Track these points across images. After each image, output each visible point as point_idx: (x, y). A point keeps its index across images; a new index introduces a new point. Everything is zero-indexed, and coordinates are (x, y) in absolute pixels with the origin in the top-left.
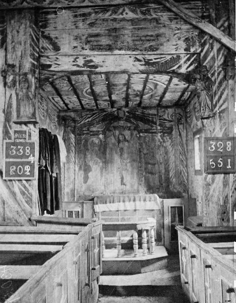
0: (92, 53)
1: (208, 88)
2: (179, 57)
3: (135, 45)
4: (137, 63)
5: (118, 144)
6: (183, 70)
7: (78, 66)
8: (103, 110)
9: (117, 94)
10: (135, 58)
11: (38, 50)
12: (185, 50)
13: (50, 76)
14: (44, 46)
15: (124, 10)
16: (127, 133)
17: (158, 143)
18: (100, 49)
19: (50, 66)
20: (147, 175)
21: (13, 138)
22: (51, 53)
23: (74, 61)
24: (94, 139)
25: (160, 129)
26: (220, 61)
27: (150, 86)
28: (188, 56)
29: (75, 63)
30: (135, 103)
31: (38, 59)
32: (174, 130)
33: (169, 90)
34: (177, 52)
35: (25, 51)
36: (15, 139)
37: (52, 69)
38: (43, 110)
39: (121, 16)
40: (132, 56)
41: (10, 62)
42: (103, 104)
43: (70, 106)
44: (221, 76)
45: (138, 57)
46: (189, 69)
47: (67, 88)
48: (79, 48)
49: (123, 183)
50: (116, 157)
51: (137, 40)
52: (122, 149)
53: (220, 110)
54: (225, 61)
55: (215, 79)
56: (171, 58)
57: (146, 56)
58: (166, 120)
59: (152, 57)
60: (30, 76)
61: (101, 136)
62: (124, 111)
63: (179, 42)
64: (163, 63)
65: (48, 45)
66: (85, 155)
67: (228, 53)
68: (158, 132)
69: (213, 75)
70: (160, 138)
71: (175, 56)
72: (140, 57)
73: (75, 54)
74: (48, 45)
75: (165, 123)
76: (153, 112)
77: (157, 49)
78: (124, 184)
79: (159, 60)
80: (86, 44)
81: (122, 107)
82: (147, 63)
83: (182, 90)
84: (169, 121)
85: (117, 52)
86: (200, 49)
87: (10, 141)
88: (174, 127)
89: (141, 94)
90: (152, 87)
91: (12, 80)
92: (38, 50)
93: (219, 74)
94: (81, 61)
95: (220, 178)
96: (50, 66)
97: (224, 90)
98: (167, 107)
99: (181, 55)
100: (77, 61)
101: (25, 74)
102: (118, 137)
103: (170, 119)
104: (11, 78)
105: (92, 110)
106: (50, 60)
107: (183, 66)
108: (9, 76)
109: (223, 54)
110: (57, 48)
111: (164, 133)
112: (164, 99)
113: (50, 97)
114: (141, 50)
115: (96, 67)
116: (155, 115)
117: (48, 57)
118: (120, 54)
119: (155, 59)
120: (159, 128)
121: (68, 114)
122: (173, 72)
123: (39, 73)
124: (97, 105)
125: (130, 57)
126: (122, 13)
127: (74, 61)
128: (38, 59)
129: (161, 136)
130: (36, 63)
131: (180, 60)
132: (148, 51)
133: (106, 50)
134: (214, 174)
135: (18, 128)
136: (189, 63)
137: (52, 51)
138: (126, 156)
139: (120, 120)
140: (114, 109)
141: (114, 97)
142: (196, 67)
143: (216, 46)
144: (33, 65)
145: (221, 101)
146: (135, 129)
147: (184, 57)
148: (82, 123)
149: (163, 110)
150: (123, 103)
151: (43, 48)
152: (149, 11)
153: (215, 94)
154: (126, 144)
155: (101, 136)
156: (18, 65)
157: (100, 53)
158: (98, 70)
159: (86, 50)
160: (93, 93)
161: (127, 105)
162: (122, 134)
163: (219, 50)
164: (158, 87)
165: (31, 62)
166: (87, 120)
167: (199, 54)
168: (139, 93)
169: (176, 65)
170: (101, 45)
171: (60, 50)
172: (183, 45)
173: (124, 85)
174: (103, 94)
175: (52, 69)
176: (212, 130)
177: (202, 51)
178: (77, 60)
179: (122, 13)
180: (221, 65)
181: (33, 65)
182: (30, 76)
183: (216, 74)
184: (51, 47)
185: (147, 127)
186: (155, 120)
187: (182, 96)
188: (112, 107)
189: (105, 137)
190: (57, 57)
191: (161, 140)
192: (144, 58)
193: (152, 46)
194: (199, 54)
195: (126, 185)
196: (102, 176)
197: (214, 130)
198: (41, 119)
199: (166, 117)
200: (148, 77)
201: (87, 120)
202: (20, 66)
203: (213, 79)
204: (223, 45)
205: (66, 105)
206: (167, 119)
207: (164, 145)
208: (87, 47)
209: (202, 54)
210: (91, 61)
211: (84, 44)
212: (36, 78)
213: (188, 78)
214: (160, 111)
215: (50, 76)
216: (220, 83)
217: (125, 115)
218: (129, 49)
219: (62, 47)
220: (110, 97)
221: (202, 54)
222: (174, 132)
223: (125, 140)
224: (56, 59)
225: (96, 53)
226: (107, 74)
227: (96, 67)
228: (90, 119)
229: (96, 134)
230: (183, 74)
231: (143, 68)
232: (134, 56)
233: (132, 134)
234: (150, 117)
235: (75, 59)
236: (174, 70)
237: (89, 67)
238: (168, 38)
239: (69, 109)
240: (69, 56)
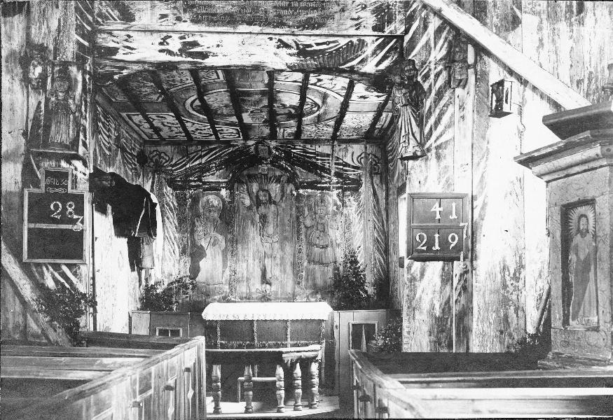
0: (195, 28)
1: (415, 101)
2: (362, 43)
3: (280, 16)
4: (284, 51)
5: (257, 208)
6: (370, 68)
7: (170, 53)
8: (228, 144)
9: (252, 112)
10: (280, 40)
11: (90, 18)
12: (374, 29)
13: (116, 70)
14: (104, 11)
16: (275, 188)
17: (331, 208)
18: (212, 20)
19: (115, 51)
20: (312, 266)
21: (43, 185)
22: (117, 26)
23: (161, 44)
24: (211, 197)
25: (338, 183)
26: (438, 53)
27: (312, 97)
28: (382, 39)
30: (289, 131)
31: (90, 36)
32: (363, 185)
33: (350, 109)
34: (358, 32)
35: (65, 21)
36: (46, 186)
37: (119, 56)
38: (109, 137)
40: (273, 37)
41: (37, 38)
42: (228, 133)
43: (165, 133)
44: (440, 82)
45: (284, 38)
46: (383, 66)
47: (154, 97)
48: (171, 18)
49: (264, 280)
50: (252, 232)
51: (283, 8)
52: (264, 218)
53: (438, 142)
54: (449, 53)
55: (430, 86)
56: (347, 44)
57: (299, 38)
58: (348, 165)
59: (309, 39)
60: (74, 69)
61: (224, 192)
62: (269, 147)
63: (362, 14)
65: (110, 11)
66: (193, 224)
67: (454, 37)
68: (333, 188)
69: (426, 77)
70: (335, 198)
71: (355, 40)
72: (288, 40)
73: (163, 28)
74: (110, 11)
75: (346, 171)
76: (326, 149)
77: (320, 26)
78: (267, 283)
79: (324, 47)
80: (185, 11)
81: (264, 138)
82: (303, 51)
83: (375, 109)
84: (353, 167)
85: (243, 28)
86: (403, 28)
87: (36, 191)
88: (363, 179)
89: (298, 113)
90: (319, 102)
91: (40, 74)
92: (90, 18)
93: (437, 75)
94: (175, 44)
95: (435, 268)
96: (115, 51)
97: (446, 105)
98: (350, 141)
99: (366, 39)
100: (168, 44)
101: (65, 65)
102: (257, 197)
103: (357, 164)
104: (39, 70)
105: (210, 143)
106: (115, 39)
107: (369, 59)
108: (35, 67)
109: (446, 39)
110: (127, 17)
111: (344, 190)
112: (343, 126)
113: (124, 114)
114: (289, 27)
115: (204, 55)
117: (110, 33)
118: (250, 33)
120: (335, 179)
121: (161, 149)
122: (352, 70)
123: (94, 63)
124: (215, 132)
125: (271, 39)
127: (161, 44)
128: (90, 36)
129: (338, 195)
130: (86, 44)
131: (365, 49)
132: (304, 28)
133: (224, 24)
134: (424, 260)
135: (48, 164)
137: (119, 21)
138: (270, 229)
139: (261, 163)
140: (250, 143)
141: (247, 118)
142: (395, 63)
143: (434, 23)
144: (80, 45)
145: (440, 128)
146: (289, 181)
147: (373, 42)
148: (188, 166)
149: (344, 146)
150: (267, 131)
151: (100, 15)
153: (430, 113)
154: (273, 207)
155: (224, 192)
156: (51, 47)
157: (212, 29)
158: (209, 62)
159: (185, 21)
160: (205, 109)
161: (273, 135)
162: (263, 190)
163: (439, 31)
164: (329, 100)
165: (78, 43)
166: (197, 162)
167: (401, 38)
168: (293, 111)
169: (357, 57)
170: (215, 15)
171: (134, 20)
172: (369, 19)
173: (263, 93)
174: (225, 111)
175: (119, 56)
177: (407, 31)
178: (168, 40)
180: (441, 60)
181: (80, 45)
182: (74, 69)
183: (432, 76)
184: (115, 14)
185: (312, 177)
186: (327, 166)
187: (376, 119)
188: (246, 138)
189: (232, 195)
190: (131, 33)
191: (339, 203)
192: (295, 42)
193: (311, 18)
194: (401, 38)
195: (270, 284)
196: (225, 265)
197: (426, 179)
198: (105, 154)
199: (348, 160)
200: (306, 79)
201: (197, 162)
202: (56, 49)
203: (426, 86)
204: (446, 23)
205: (157, 130)
206: (352, 164)
207: (345, 211)
208: (187, 16)
209: (407, 38)
210: (195, 44)
211: (182, 11)
212: (84, 72)
213: (379, 82)
214: (337, 148)
215: (116, 70)
216: (440, 95)
218: (267, 23)
219: (137, 16)
220: (240, 119)
221: (407, 38)
222: (362, 189)
223: (271, 201)
224: (126, 37)
225: (203, 28)
226: (227, 70)
227: (204, 55)
228: (203, 161)
229: (215, 188)
230: (370, 74)
231: (294, 60)
232: (278, 37)
233: (283, 190)
234: (318, 160)
235: (164, 39)
236: (352, 67)
237: (190, 55)
238: (342, 6)
239: (162, 139)
240: (152, 32)
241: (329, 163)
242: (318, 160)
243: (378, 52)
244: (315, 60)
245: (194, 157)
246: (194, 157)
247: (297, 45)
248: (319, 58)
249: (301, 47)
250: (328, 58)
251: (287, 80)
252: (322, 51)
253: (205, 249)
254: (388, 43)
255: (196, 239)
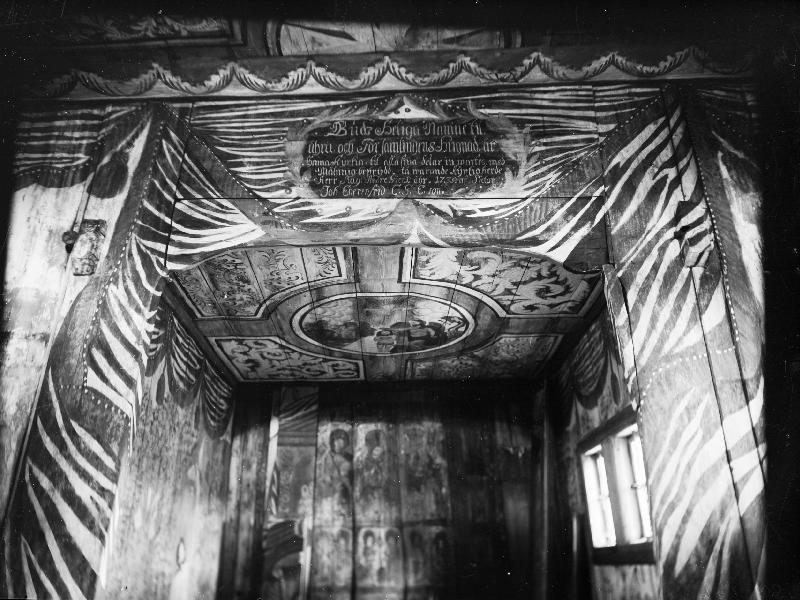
15: (401, 104)
29: (268, 218)
39: (393, 116)
64: (502, 220)
82: (462, 219)
119: (483, 210)
126: (395, 110)
136: (574, 220)
152: (465, 105)
176: (666, 406)
179: (395, 110)
210: (313, 214)
243: (571, 217)
244: (479, 229)
247: (454, 211)
248: (485, 226)
249: (460, 214)
250: (498, 227)
251: (433, 277)
252: (491, 219)
254: (583, 206)
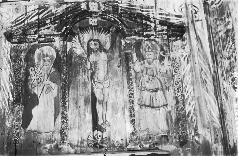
5: (88, 56)
84: (176, 16)
103: (179, 13)
116: (152, 7)
120: (159, 28)
148: (26, 22)
154: (103, 56)
217: (99, 8)
228: (41, 16)
229: (49, 41)
241: (153, 14)
242: (143, 11)
245: (32, 14)
246: (32, 14)
253: (38, 97)
255: (30, 87)
